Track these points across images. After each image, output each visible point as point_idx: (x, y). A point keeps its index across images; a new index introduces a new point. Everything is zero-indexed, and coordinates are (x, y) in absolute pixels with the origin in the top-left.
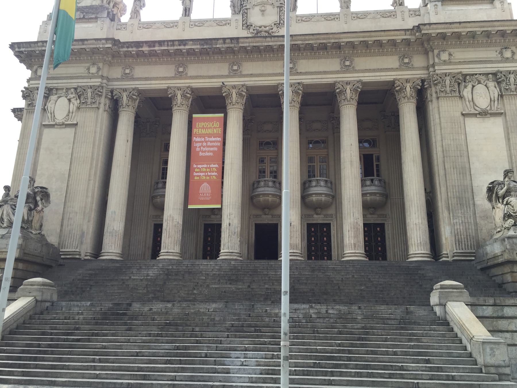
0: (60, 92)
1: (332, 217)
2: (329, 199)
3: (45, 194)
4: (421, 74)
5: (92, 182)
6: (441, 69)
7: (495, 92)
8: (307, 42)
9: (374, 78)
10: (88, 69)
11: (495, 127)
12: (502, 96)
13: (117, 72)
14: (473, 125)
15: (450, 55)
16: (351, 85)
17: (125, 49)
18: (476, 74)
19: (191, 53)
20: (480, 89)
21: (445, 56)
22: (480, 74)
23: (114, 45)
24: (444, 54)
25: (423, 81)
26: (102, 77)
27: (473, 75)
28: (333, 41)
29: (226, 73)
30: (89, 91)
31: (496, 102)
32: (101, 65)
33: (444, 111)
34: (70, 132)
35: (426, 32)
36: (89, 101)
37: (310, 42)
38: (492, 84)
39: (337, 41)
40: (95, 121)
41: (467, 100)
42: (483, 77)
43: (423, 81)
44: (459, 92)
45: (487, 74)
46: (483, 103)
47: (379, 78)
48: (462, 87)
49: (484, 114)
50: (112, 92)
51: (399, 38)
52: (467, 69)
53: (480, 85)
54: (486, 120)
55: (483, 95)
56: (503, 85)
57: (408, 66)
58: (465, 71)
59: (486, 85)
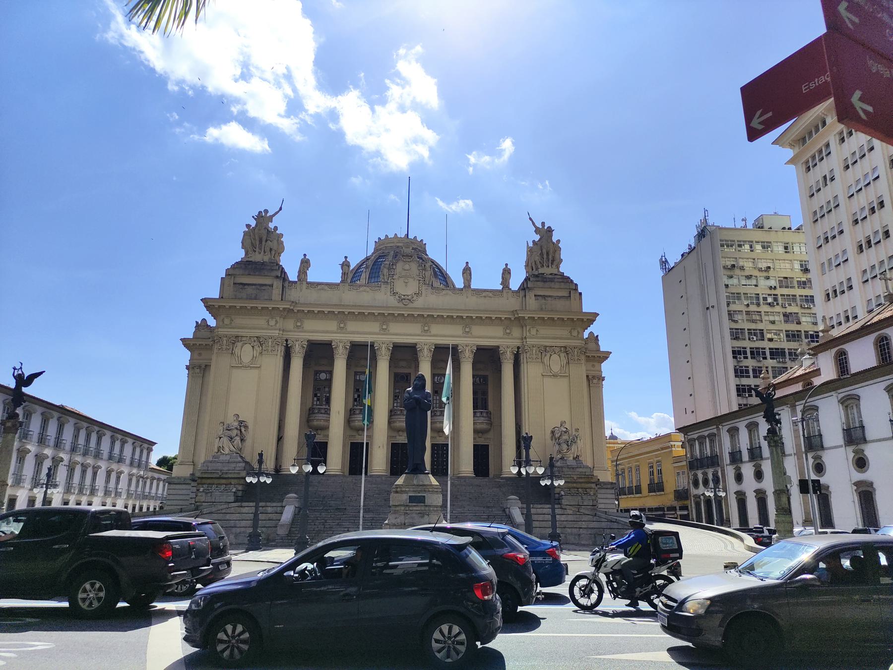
0: (244, 339)
3: (242, 425)
4: (518, 343)
6: (530, 341)
10: (268, 322)
13: (290, 324)
20: (555, 357)
21: (533, 332)
25: (518, 348)
29: (377, 330)
32: (278, 318)
33: (531, 371)
36: (270, 348)
38: (562, 355)
40: (273, 364)
42: (558, 349)
43: (518, 348)
46: (556, 368)
49: (555, 376)
50: (287, 341)
51: (503, 317)
52: (548, 342)
55: (556, 362)
58: (547, 344)
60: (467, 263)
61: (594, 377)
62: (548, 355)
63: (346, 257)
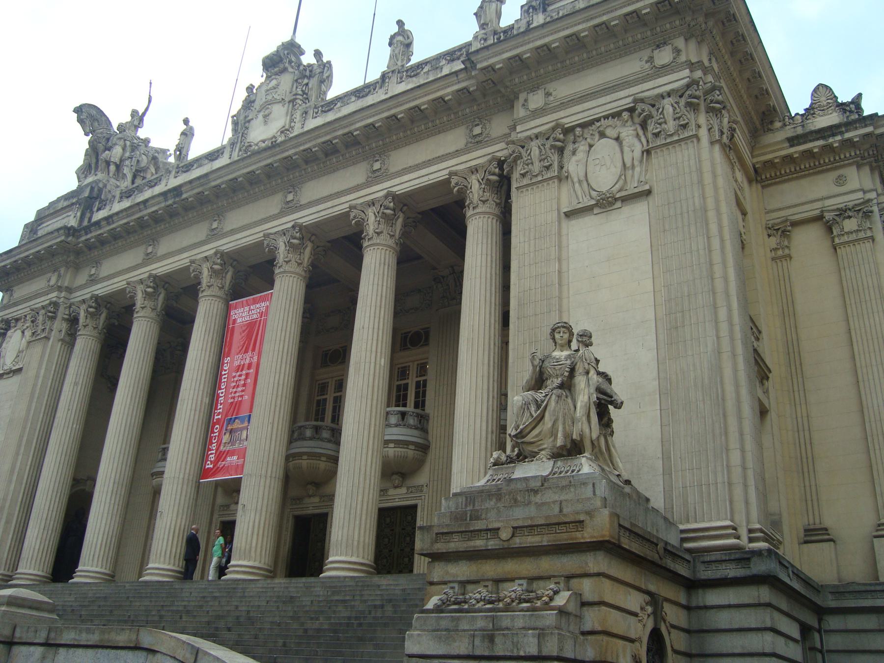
1: (422, 491)
2: (410, 453)
4: (499, 150)
5: (20, 457)
6: (523, 130)
7: (634, 146)
8: (302, 148)
9: (417, 181)
11: (632, 226)
12: (648, 152)
14: (584, 235)
15: (548, 94)
16: (378, 206)
17: (83, 238)
18: (598, 120)
19: (156, 219)
20: (605, 148)
21: (536, 100)
22: (606, 117)
23: (68, 235)
24: (536, 97)
25: (501, 163)
26: (60, 289)
27: (591, 123)
28: (340, 132)
30: (42, 312)
31: (637, 169)
32: (62, 270)
34: (16, 379)
35: (485, 64)
37: (307, 146)
38: (628, 132)
39: (346, 130)
41: (576, 180)
44: (561, 167)
45: (617, 115)
46: (605, 179)
47: (426, 179)
48: (567, 152)
49: (606, 203)
52: (571, 116)
53: (604, 140)
54: (614, 215)
56: (651, 127)
57: (477, 142)
58: (568, 122)
59: (617, 139)
60: (400, 23)
61: (843, 213)
62: (582, 147)
63: (186, 122)
